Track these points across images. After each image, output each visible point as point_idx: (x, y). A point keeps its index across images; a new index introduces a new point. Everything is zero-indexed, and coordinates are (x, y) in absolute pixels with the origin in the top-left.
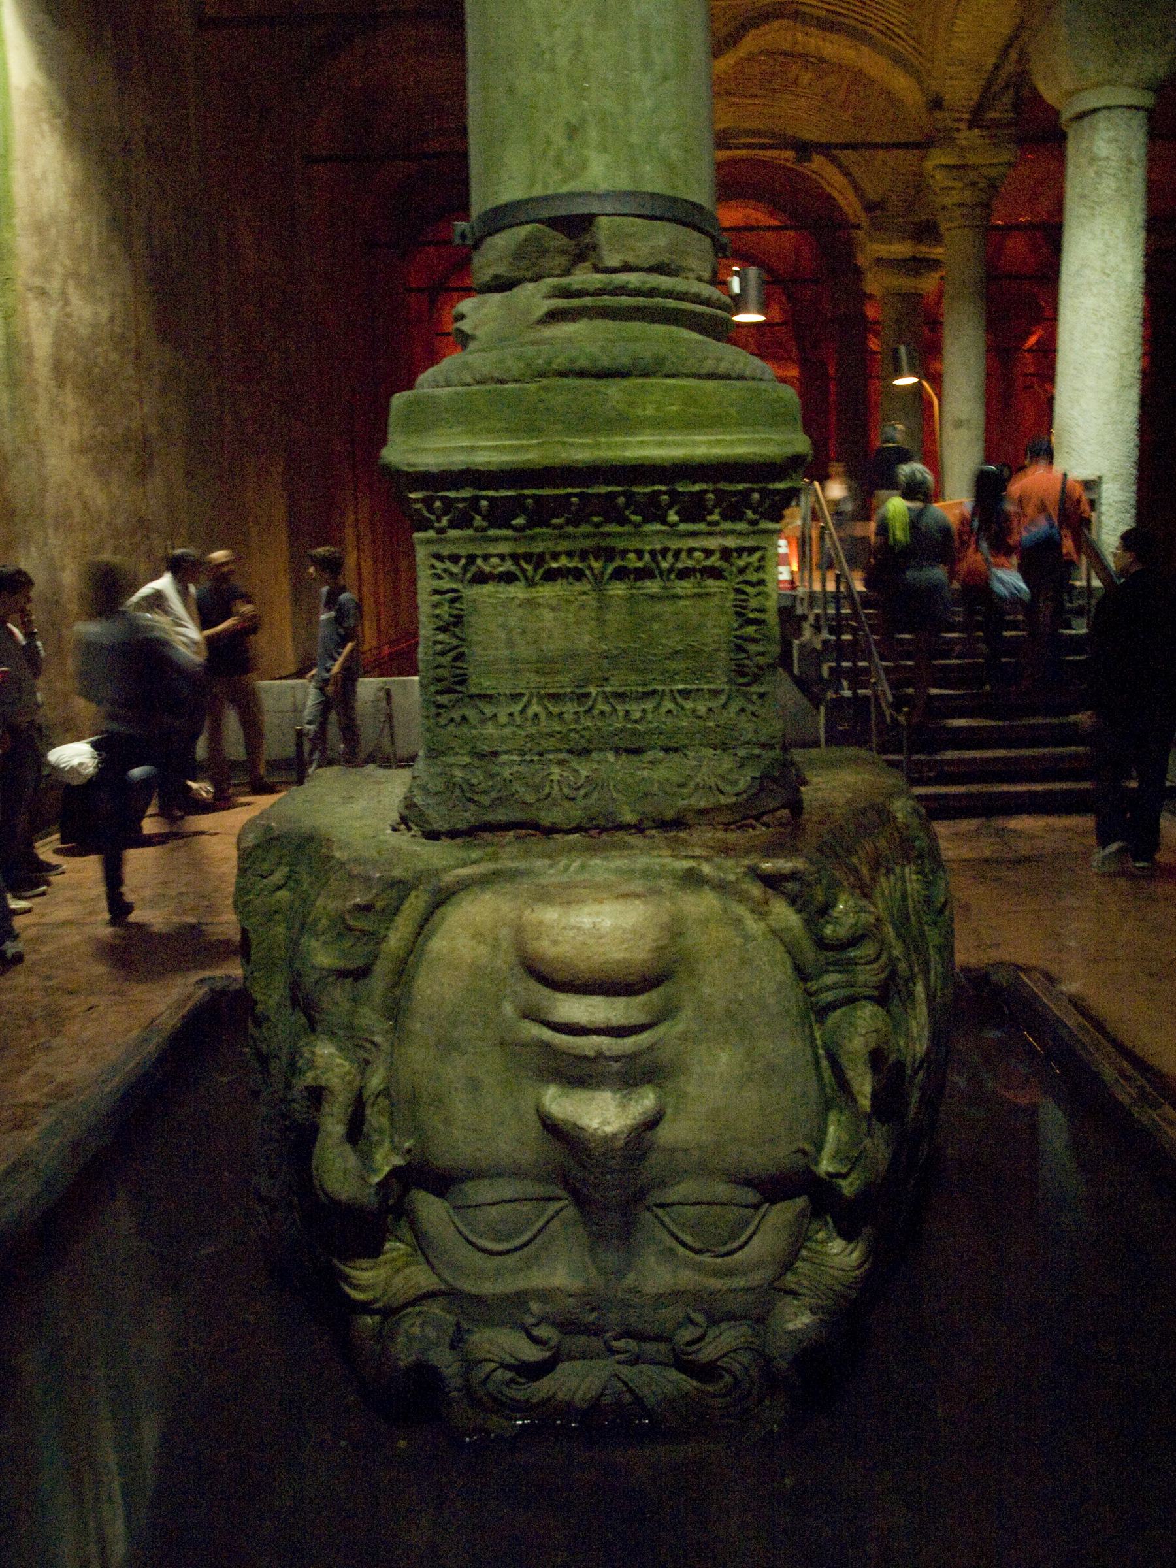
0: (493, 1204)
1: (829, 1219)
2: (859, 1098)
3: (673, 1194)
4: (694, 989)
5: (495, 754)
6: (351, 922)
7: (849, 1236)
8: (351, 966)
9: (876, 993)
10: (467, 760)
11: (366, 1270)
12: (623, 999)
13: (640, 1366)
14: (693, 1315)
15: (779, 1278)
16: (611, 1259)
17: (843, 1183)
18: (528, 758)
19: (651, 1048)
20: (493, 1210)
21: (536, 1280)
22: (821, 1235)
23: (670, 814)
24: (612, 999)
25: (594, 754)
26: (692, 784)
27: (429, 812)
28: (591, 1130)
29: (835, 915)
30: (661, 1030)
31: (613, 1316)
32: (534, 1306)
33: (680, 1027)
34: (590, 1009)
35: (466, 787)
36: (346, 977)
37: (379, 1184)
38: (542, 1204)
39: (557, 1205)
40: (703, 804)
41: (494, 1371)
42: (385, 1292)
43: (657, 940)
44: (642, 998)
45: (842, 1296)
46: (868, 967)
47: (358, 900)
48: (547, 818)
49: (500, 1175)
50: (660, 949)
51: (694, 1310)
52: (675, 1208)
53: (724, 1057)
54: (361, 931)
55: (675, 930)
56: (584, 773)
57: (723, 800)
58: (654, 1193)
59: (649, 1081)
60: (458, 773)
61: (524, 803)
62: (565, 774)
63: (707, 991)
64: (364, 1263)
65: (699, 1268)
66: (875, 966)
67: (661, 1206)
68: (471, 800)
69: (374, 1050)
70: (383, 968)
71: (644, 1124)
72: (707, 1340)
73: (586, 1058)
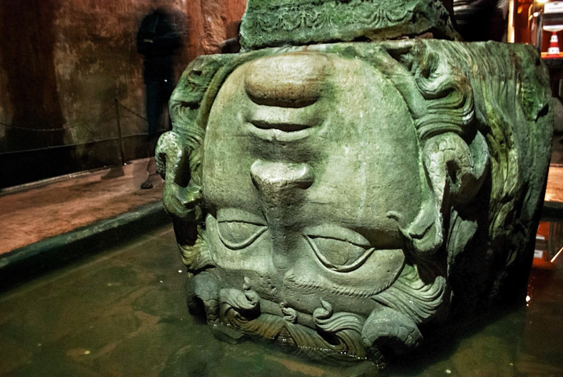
0: (230, 222)
1: (416, 267)
2: (437, 190)
3: (317, 230)
4: (333, 108)
5: (278, 7)
6: (190, 79)
7: (428, 280)
8: (187, 100)
9: (460, 130)
10: (264, 11)
11: (188, 250)
12: (289, 109)
13: (298, 325)
14: (323, 302)
15: (377, 294)
16: (281, 260)
17: (418, 241)
18: (292, 8)
19: (305, 139)
20: (231, 225)
21: (247, 265)
22: (410, 276)
23: (360, 33)
24: (283, 109)
25: (325, 5)
26: (373, 16)
27: (246, 37)
28: (263, 180)
29: (435, 75)
30: (312, 130)
31: (282, 294)
32: (246, 279)
33: (323, 130)
34: (272, 113)
35: (262, 24)
36: (186, 107)
37: (185, 204)
38: (255, 226)
39: (263, 228)
40: (377, 27)
41: (230, 308)
42: (193, 262)
43: (308, 75)
44: (302, 110)
45: (416, 314)
46: (455, 111)
47: (194, 69)
48: (296, 38)
49: (234, 207)
50: (311, 80)
51: (324, 299)
52: (319, 239)
53: (347, 150)
54: (194, 83)
55: (324, 74)
56: (317, 13)
57: (390, 24)
58: (307, 229)
59: (305, 162)
60: (259, 17)
61: (288, 30)
62: (308, 14)
63: (341, 109)
64: (188, 248)
65: (327, 276)
66: (460, 110)
67: (313, 237)
68: (263, 30)
69: (196, 143)
70: (203, 104)
71: (298, 183)
72: (332, 318)
73: (268, 141)
